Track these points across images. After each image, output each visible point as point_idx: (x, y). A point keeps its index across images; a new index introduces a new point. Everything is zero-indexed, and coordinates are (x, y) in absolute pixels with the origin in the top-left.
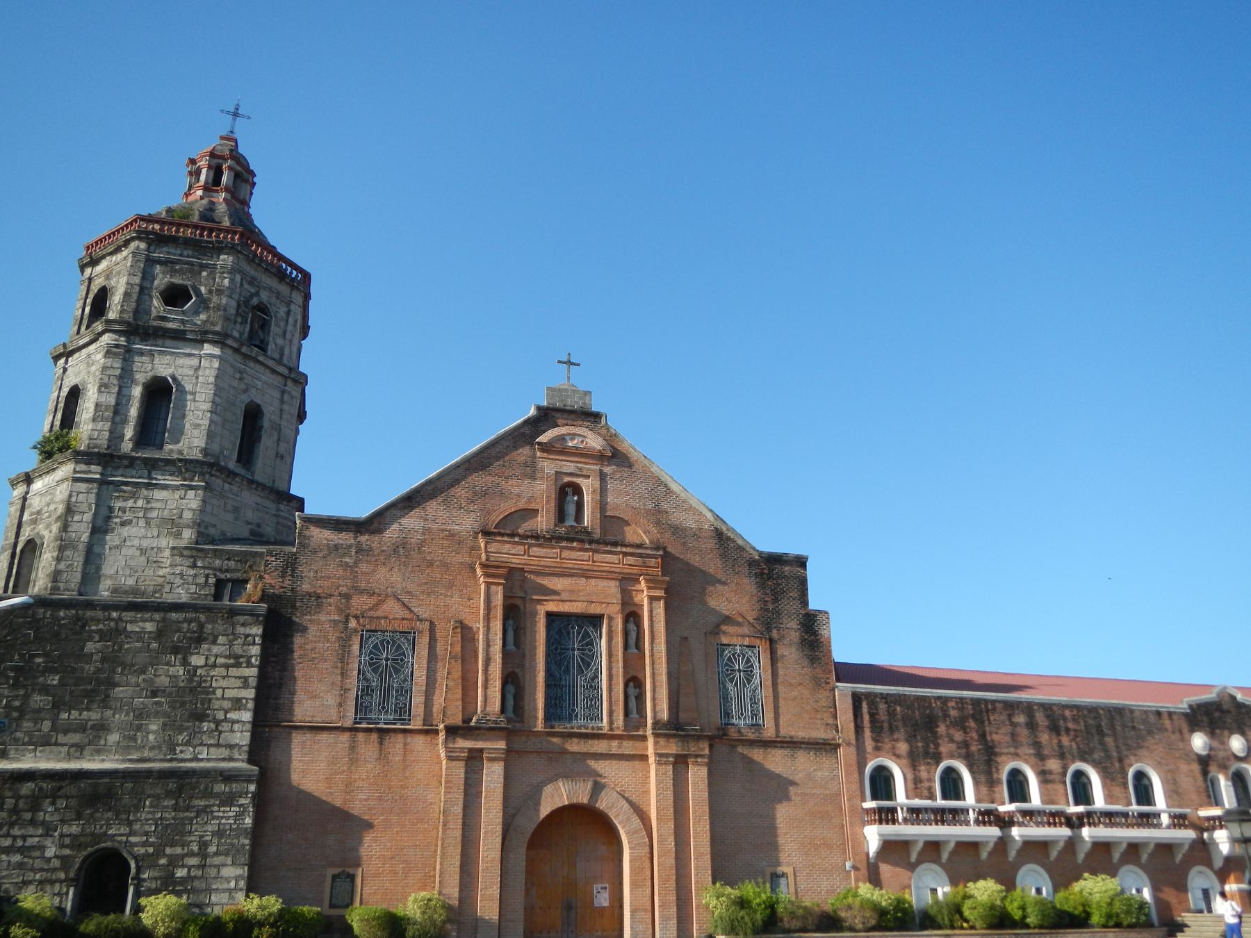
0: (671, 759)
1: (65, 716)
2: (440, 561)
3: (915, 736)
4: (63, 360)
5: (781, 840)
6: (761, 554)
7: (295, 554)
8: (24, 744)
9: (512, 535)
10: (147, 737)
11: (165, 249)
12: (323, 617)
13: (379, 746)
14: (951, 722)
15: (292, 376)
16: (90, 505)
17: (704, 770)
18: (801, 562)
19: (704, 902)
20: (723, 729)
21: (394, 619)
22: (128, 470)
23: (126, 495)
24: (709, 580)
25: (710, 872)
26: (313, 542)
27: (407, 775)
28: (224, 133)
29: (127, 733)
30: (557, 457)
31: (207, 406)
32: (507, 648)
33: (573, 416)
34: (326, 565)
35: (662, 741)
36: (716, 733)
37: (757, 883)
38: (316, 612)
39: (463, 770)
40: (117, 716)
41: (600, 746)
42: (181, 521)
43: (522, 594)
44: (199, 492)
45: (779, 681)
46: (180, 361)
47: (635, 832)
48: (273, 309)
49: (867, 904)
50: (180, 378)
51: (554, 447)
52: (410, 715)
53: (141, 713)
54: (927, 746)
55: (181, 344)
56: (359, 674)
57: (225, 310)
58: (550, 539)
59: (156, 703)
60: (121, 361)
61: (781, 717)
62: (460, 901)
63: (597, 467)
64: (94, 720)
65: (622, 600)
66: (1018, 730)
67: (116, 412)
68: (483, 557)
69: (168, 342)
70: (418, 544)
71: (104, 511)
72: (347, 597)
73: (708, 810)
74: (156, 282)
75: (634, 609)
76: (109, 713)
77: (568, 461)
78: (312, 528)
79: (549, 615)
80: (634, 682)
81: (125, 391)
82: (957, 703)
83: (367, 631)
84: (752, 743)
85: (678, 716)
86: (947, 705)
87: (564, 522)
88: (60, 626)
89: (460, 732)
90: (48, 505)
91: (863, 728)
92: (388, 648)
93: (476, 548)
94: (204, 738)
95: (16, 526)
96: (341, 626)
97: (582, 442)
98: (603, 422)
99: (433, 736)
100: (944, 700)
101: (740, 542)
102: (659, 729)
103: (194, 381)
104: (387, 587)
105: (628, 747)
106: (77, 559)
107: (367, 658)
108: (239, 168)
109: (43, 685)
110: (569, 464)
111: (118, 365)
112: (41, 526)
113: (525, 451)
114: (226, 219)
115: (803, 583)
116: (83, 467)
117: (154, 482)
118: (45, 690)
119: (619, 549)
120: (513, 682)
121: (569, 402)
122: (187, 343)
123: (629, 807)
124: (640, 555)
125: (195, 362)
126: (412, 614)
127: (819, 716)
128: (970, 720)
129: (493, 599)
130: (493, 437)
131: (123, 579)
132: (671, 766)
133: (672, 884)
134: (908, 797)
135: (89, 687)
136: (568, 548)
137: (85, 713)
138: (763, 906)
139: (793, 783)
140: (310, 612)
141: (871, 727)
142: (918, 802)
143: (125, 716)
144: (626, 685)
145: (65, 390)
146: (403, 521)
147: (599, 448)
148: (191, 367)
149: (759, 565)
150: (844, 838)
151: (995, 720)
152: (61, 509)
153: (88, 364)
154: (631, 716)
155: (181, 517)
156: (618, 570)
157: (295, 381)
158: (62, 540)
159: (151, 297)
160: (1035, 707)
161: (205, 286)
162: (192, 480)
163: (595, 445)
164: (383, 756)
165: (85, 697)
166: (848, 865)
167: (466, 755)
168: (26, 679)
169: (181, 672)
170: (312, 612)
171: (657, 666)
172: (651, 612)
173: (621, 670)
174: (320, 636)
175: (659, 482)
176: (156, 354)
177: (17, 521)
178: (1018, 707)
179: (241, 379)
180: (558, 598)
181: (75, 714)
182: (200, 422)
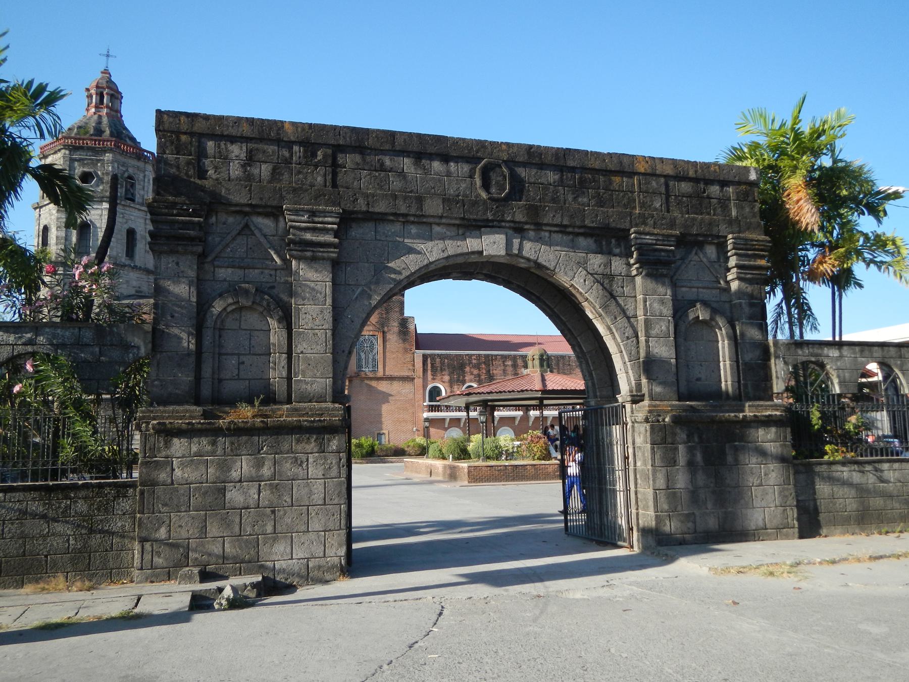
4: (38, 210)
5: (383, 420)
11: (78, 153)
28: (103, 70)
37: (367, 438)
48: (135, 177)
54: (459, 377)
66: (507, 368)
67: (66, 239)
84: (371, 379)
108: (113, 92)
111: (64, 216)
114: (107, 129)
125: (99, 212)
139: (391, 395)
145: (41, 227)
166: (414, 429)
179: (123, 217)
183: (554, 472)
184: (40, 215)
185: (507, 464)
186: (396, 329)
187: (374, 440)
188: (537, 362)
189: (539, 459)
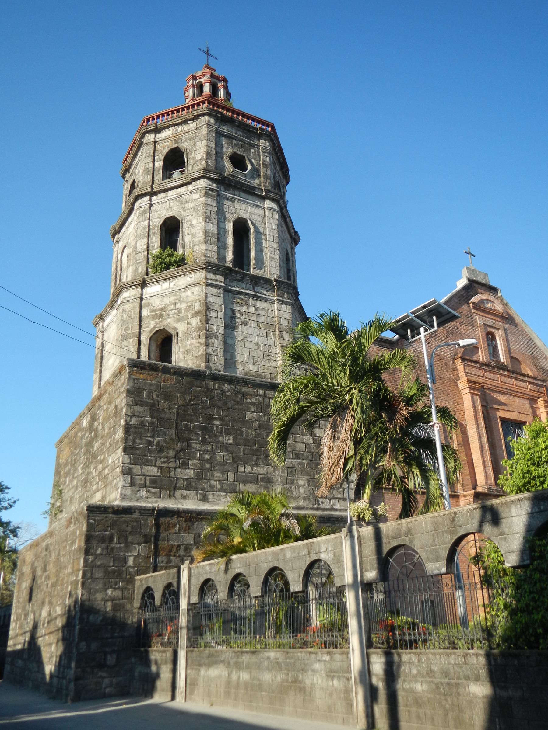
1: (241, 469)
8: (218, 491)
10: (299, 491)
15: (296, 238)
16: (220, 305)
22: (240, 283)
23: (241, 302)
29: (285, 486)
30: (481, 314)
31: (276, 246)
33: (483, 288)
40: (276, 472)
42: (281, 327)
43: (485, 404)
44: (289, 306)
46: (253, 210)
50: (254, 221)
53: (292, 471)
55: (250, 197)
57: (270, 179)
58: (494, 368)
59: (300, 464)
60: (216, 202)
63: (501, 324)
64: (262, 474)
67: (218, 239)
68: (462, 374)
69: (242, 194)
71: (230, 313)
74: (224, 150)
76: (271, 469)
77: (487, 317)
81: (222, 225)
88: (226, 396)
89: (481, 497)
90: (175, 304)
93: (455, 369)
94: (334, 492)
95: (138, 319)
98: (499, 294)
99: (457, 499)
103: (263, 226)
106: (218, 345)
109: (223, 443)
111: (215, 204)
112: (169, 320)
113: (465, 307)
116: (210, 276)
117: (259, 295)
118: (225, 447)
119: (526, 379)
122: (254, 198)
124: (536, 384)
125: (261, 212)
129: (476, 405)
130: (450, 295)
131: (250, 366)
135: (255, 448)
137: (255, 468)
143: (282, 473)
145: (157, 221)
147: (501, 311)
148: (260, 215)
152: (198, 306)
153: (181, 202)
155: (280, 324)
156: (528, 393)
158: (206, 330)
159: (222, 159)
161: (255, 159)
162: (283, 297)
165: (253, 455)
168: (210, 437)
169: (311, 441)
175: (531, 340)
176: (236, 201)
177: (138, 316)
181: (248, 468)
182: (274, 256)
184: (151, 205)
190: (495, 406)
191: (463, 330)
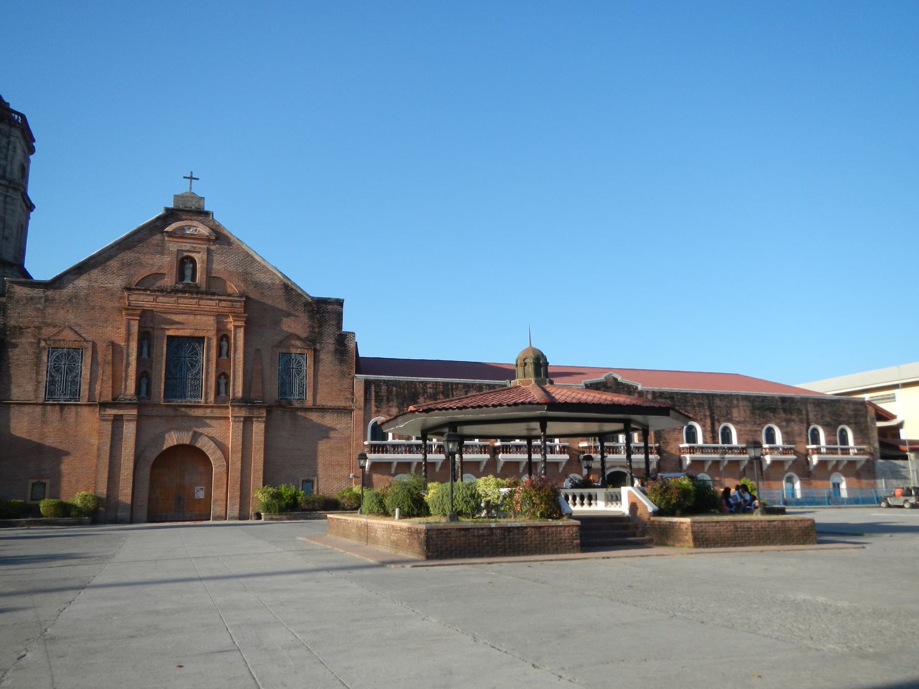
0: (242, 419)
2: (100, 306)
3: (403, 404)
6: (312, 298)
7: (5, 303)
9: (145, 290)
12: (24, 340)
13: (60, 414)
14: (427, 396)
15: (12, 185)
17: (263, 425)
18: (340, 303)
19: (255, 496)
20: (279, 402)
21: (70, 341)
24: (276, 314)
25: (262, 480)
26: (16, 296)
27: (78, 429)
32: (143, 357)
33: (189, 214)
34: (25, 309)
35: (236, 409)
36: (275, 404)
37: (288, 486)
38: (19, 337)
39: (110, 426)
41: (199, 412)
43: (151, 325)
45: (319, 374)
47: (218, 459)
49: (352, 495)
51: (176, 234)
52: (79, 396)
56: (47, 373)
58: (170, 292)
61: (318, 394)
62: (108, 496)
63: (205, 247)
65: (218, 328)
70: (85, 296)
72: (39, 328)
73: (263, 447)
75: (226, 333)
77: (186, 243)
78: (15, 286)
79: (169, 337)
80: (223, 376)
82: (433, 385)
83: (52, 348)
85: (250, 395)
86: (426, 387)
87: (183, 281)
91: (370, 400)
92: (65, 357)
96: (35, 345)
97: (196, 230)
98: (211, 218)
99: (94, 407)
100: (425, 383)
101: (299, 291)
102: (235, 403)
104: (65, 322)
105: (217, 413)
107: (52, 364)
110: (187, 244)
113: (158, 237)
115: (340, 315)
119: (216, 297)
120: (144, 376)
121: (189, 204)
123: (215, 446)
124: (231, 301)
126: (81, 338)
127: (342, 394)
128: (440, 395)
130: (135, 228)
132: (242, 423)
133: (238, 486)
134: (394, 438)
136: (181, 297)
138: (289, 497)
140: (16, 337)
141: (375, 400)
142: (397, 441)
144: (218, 378)
146: (76, 282)
147: (207, 234)
149: (311, 305)
150: (350, 461)
151: (456, 394)
154: (221, 395)
156: (215, 310)
157: (14, 189)
160: (484, 387)
163: (204, 232)
164: (62, 419)
167: (112, 418)
170: (17, 337)
171: (237, 367)
172: (235, 335)
173: (214, 370)
174: (22, 352)
175: (247, 255)
178: (473, 387)
180: (174, 327)
183: (572, 539)
185: (493, 525)
186: (331, 347)
187: (297, 488)
188: (530, 369)
189: (542, 515)
190: (163, 326)
191: (146, 260)
